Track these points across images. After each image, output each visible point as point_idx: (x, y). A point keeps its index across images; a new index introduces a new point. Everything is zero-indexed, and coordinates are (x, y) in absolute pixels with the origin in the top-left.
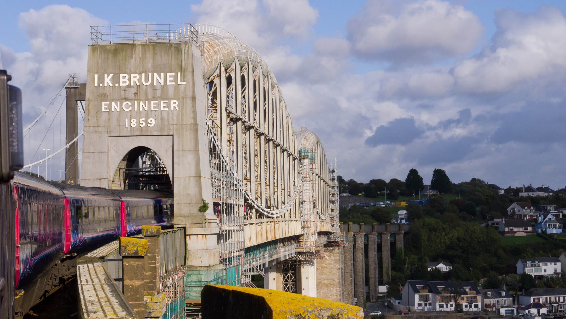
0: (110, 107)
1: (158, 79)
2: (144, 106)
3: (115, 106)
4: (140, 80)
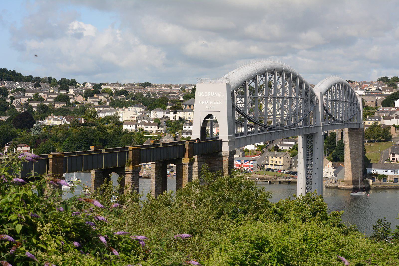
0: (202, 102)
1: (216, 94)
2: (211, 102)
3: (203, 102)
4: (211, 94)
